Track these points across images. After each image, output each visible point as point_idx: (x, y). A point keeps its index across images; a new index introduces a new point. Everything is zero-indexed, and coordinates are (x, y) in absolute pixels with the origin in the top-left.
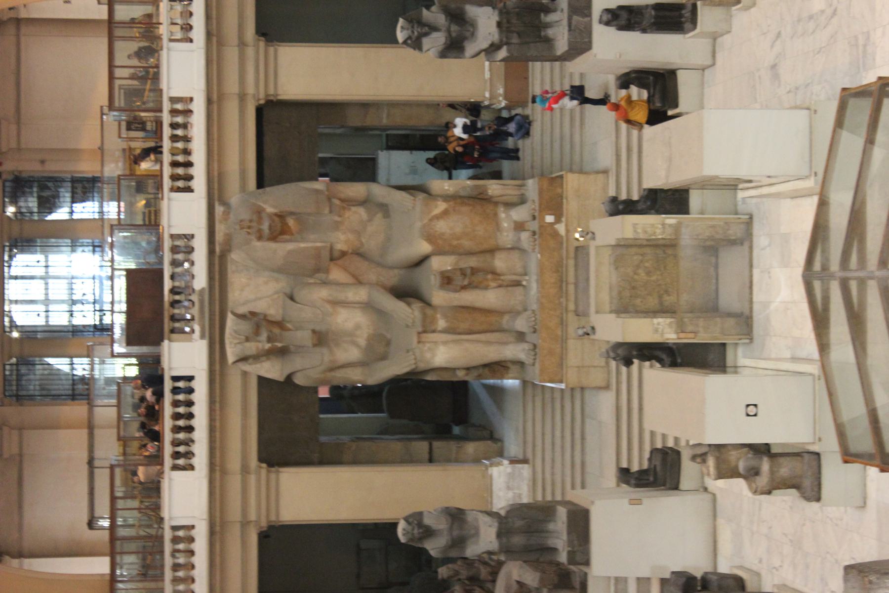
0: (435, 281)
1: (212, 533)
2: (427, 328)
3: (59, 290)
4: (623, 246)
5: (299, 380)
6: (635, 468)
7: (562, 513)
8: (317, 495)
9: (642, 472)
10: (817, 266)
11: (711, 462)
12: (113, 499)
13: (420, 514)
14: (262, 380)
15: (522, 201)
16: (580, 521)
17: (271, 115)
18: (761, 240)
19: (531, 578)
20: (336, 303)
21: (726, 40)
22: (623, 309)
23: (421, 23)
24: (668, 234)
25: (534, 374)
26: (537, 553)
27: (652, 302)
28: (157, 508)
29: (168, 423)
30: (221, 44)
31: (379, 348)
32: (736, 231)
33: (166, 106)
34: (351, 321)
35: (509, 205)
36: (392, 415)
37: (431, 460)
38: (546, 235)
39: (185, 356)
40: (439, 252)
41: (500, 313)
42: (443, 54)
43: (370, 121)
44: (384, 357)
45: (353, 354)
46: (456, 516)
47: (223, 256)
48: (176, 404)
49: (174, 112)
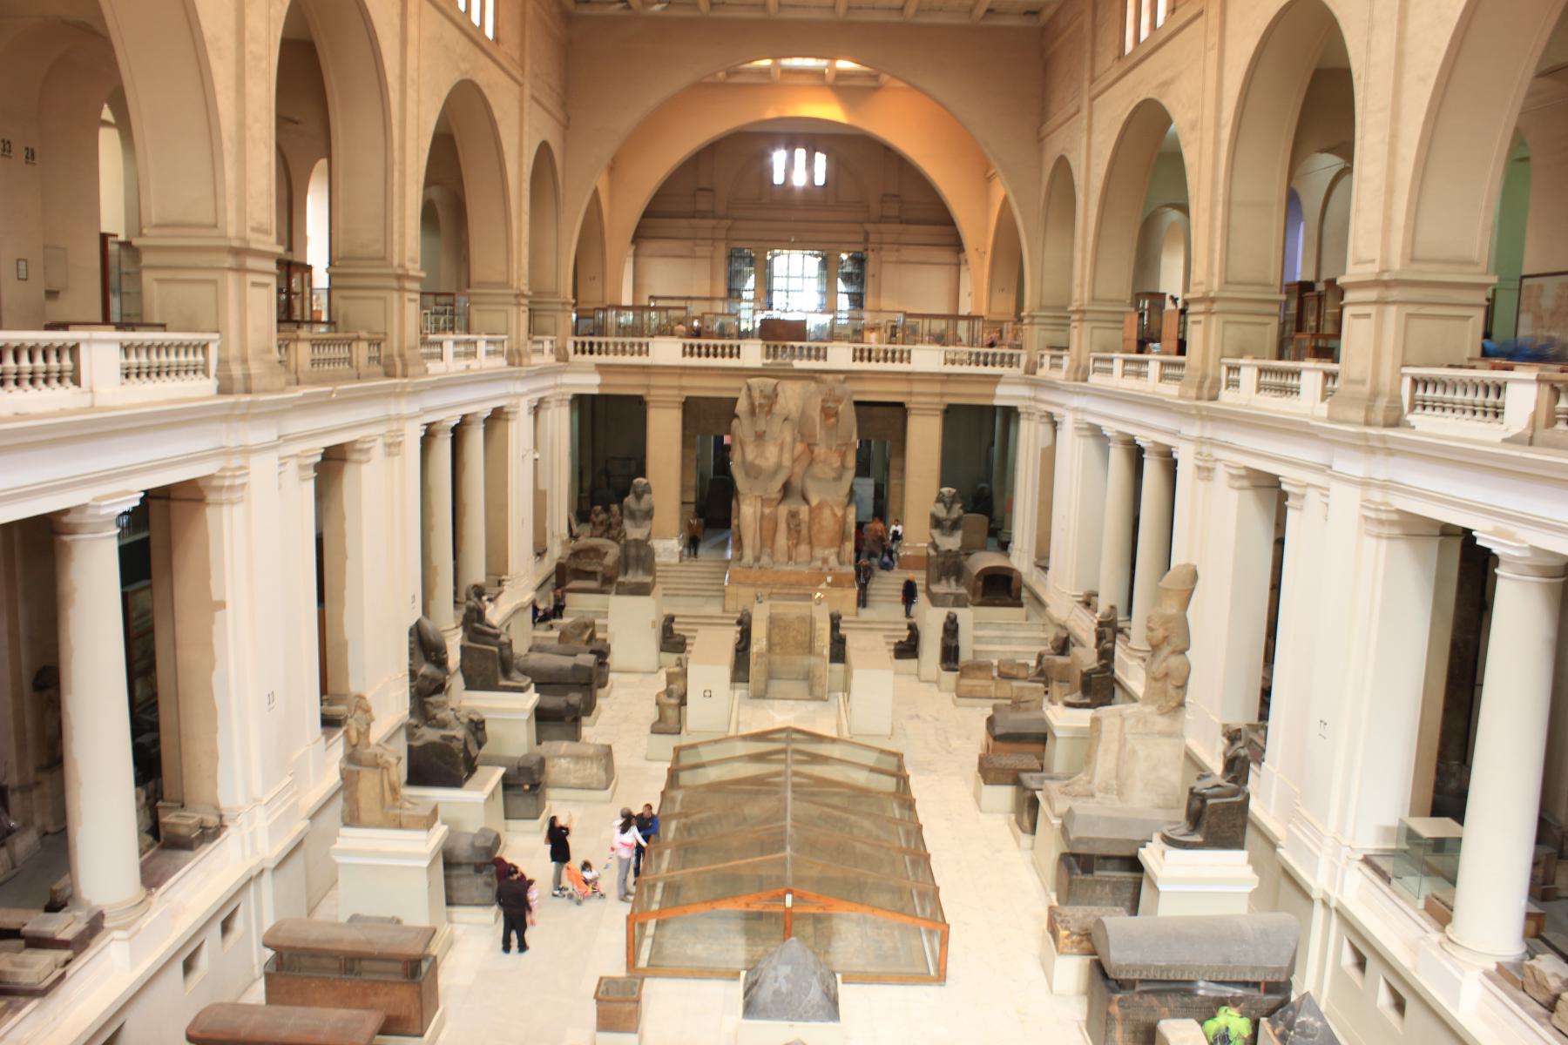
0: (793, 507)
2: (765, 502)
3: (795, 284)
4: (811, 622)
5: (735, 422)
6: (675, 626)
7: (648, 579)
8: (664, 434)
9: (671, 630)
10: (795, 736)
11: (677, 669)
12: (667, 309)
13: (649, 491)
14: (735, 400)
15: (841, 563)
16: (642, 590)
18: (812, 706)
19: (610, 560)
20: (782, 447)
21: (935, 688)
22: (773, 621)
23: (953, 502)
24: (817, 650)
25: (734, 567)
26: (624, 564)
27: (776, 639)
30: (942, 382)
31: (753, 472)
32: (818, 691)
33: (906, 347)
34: (770, 456)
35: (839, 555)
36: (712, 481)
37: (683, 503)
38: (818, 577)
39: (752, 354)
40: (811, 511)
43: (893, 472)
44: (747, 475)
46: (648, 514)
47: (812, 378)
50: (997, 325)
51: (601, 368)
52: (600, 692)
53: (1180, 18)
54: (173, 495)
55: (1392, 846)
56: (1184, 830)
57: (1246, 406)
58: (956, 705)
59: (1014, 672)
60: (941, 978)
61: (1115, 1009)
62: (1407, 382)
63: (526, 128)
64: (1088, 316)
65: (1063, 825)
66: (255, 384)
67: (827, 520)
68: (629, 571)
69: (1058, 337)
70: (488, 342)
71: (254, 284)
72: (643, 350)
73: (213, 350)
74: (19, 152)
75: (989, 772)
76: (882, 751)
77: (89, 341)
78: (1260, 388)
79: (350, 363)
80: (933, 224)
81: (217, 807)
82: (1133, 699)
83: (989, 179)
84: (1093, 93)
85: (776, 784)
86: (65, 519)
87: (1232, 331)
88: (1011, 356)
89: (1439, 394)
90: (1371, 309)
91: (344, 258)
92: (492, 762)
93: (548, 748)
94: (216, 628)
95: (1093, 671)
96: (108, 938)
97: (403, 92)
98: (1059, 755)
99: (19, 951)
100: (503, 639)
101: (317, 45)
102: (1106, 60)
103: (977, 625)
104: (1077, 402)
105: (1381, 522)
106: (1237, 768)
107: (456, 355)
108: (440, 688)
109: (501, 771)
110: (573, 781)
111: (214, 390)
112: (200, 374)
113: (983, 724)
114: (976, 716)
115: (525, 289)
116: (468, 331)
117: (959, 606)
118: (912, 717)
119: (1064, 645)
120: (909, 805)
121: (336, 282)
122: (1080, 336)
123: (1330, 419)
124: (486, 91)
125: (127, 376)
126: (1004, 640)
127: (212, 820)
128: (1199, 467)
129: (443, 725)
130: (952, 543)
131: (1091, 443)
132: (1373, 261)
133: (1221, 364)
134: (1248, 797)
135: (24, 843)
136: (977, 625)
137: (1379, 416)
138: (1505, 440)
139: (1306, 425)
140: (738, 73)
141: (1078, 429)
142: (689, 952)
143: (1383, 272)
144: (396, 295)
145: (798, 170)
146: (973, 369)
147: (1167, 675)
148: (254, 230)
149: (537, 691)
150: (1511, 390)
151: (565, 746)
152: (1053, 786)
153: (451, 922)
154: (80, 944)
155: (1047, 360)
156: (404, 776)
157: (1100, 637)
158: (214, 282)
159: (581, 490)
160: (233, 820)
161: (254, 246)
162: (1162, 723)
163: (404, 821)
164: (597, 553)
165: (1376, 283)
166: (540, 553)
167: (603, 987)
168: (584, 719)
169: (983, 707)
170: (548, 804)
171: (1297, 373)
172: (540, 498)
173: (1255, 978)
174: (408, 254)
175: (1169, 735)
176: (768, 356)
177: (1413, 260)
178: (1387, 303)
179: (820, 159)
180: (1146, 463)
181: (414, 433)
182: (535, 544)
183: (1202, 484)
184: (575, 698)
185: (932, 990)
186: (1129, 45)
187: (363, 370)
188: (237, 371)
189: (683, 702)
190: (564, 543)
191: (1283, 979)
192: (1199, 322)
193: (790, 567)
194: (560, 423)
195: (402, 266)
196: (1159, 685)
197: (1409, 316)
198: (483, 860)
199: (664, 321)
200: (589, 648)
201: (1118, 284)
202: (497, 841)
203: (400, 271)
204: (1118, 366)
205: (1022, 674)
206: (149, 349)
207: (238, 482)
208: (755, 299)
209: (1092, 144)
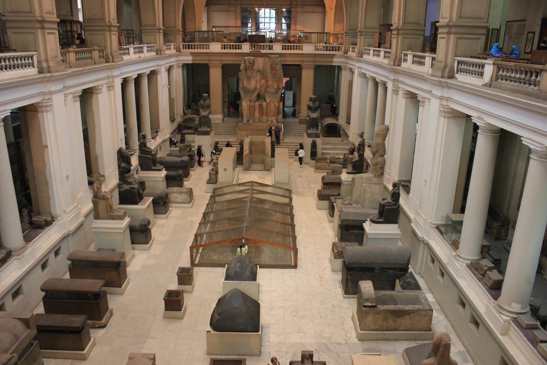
0: (261, 103)
1: (208, 53)
2: (250, 101)
3: (267, 20)
4: (263, 143)
5: (240, 73)
7: (209, 129)
8: (216, 76)
9: (218, 147)
14: (240, 64)
15: (278, 122)
16: (207, 133)
17: (299, 67)
18: (265, 172)
19: (197, 122)
21: (309, 166)
22: (251, 143)
26: (200, 124)
27: (253, 149)
29: (231, 44)
31: (247, 91)
32: (267, 168)
34: (253, 84)
35: (277, 120)
37: (223, 101)
40: (267, 104)
41: (253, 117)
42: (308, 106)
44: (244, 91)
45: (245, 85)
46: (209, 107)
47: (267, 57)
48: (236, 45)
50: (336, 36)
51: (192, 54)
52: (191, 169)
56: (376, 218)
57: (409, 69)
59: (335, 161)
60: (295, 267)
61: (349, 277)
62: (456, 62)
64: (363, 34)
66: (52, 69)
68: (204, 126)
70: (148, 47)
71: (48, 33)
72: (208, 47)
73: (35, 58)
75: (321, 197)
76: (286, 190)
78: (413, 62)
79: (92, 59)
81: (51, 214)
85: (245, 201)
88: (339, 47)
90: (445, 36)
92: (149, 195)
93: (171, 189)
94: (45, 155)
95: (356, 161)
96: (14, 258)
100: (153, 153)
103: (323, 144)
104: (358, 65)
105: (445, 112)
106: (396, 196)
107: (135, 53)
108: (129, 171)
109: (152, 198)
110: (179, 200)
112: (31, 67)
114: (320, 176)
115: (161, 27)
117: (317, 137)
118: (299, 177)
120: (292, 208)
122: (360, 40)
127: (49, 219)
129: (130, 183)
130: (315, 115)
131: (363, 79)
132: (447, 18)
136: (323, 144)
137: (446, 74)
138: (483, 85)
139: (423, 76)
142: (212, 258)
143: (450, 22)
146: (325, 52)
147: (377, 164)
150: (486, 67)
151: (176, 189)
152: (339, 201)
155: (351, 48)
156: (118, 202)
159: (189, 97)
160: (57, 218)
161: (46, 19)
162: (375, 180)
164: (192, 120)
165: (448, 26)
166: (172, 120)
169: (324, 172)
170: (170, 208)
171: (424, 57)
172: (171, 102)
173: (396, 267)
174: (111, 17)
182: (170, 118)
183: (394, 96)
185: (292, 270)
187: (97, 61)
188: (44, 65)
190: (181, 116)
191: (405, 267)
194: (178, 75)
195: (109, 22)
196: (374, 167)
197: (458, 38)
199: (215, 36)
200: (187, 154)
201: (374, 22)
202: (149, 222)
203: (109, 24)
204: (372, 52)
205: (338, 161)
206: (9, 59)
207: (48, 104)
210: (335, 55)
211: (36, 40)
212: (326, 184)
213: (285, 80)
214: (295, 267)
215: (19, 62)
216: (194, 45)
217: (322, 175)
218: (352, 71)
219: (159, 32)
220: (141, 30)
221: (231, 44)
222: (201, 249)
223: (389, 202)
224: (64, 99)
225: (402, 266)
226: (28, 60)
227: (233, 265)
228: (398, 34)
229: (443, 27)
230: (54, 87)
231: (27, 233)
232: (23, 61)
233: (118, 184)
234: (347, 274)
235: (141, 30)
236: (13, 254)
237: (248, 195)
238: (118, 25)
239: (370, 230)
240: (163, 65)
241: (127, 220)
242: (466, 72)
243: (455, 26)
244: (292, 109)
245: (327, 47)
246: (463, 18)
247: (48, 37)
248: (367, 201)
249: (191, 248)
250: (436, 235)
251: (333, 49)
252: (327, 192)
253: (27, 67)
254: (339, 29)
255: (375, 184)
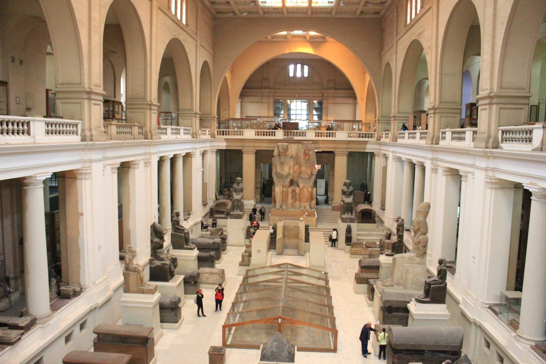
0: (294, 188)
1: (242, 139)
2: (284, 186)
3: (299, 112)
4: (297, 228)
5: (273, 158)
7: (242, 213)
8: (249, 162)
10: (289, 266)
14: (273, 151)
15: (311, 208)
16: (239, 217)
18: (298, 257)
19: (229, 207)
21: (343, 252)
22: (285, 228)
25: (273, 209)
26: (233, 209)
27: (286, 234)
28: (247, 128)
29: (265, 131)
30: (347, 144)
31: (280, 176)
32: (301, 252)
34: (286, 170)
35: (310, 205)
36: (267, 181)
37: (256, 188)
39: (280, 134)
40: (300, 190)
43: (331, 176)
44: (278, 177)
45: (279, 170)
46: (241, 190)
48: (269, 132)
49: (332, 133)
50: (368, 125)
51: (226, 140)
52: (223, 252)
53: (424, 10)
54: (66, 176)
55: (499, 303)
56: (422, 297)
57: (449, 145)
58: (350, 257)
60: (335, 350)
61: (396, 361)
62: (500, 132)
63: (198, 56)
65: (381, 296)
66: (94, 138)
67: (306, 193)
69: (387, 127)
70: (184, 130)
71: (94, 104)
73: (80, 126)
74: (17, 62)
75: (359, 280)
77: (34, 121)
78: (453, 139)
79: (131, 134)
80: (346, 90)
81: (80, 285)
82: (409, 251)
83: (365, 73)
84: (397, 39)
86: (25, 181)
87: (443, 119)
88: (372, 134)
89: (511, 135)
90: (487, 107)
91: (131, 98)
94: (80, 223)
95: (396, 243)
97: (151, 41)
98: (382, 271)
99: (6, 330)
100: (186, 231)
101: (122, 25)
102: (401, 27)
103: (358, 230)
105: (492, 183)
106: (442, 274)
107: (172, 133)
108: (161, 247)
109: (183, 277)
111: (80, 140)
112: (75, 134)
113: (358, 262)
115: (198, 111)
116: (178, 125)
118: (334, 261)
119: (389, 237)
120: (328, 290)
121: (128, 107)
123: (475, 147)
124: (183, 43)
125: (48, 133)
126: (368, 235)
127: (78, 289)
128: (432, 169)
129: (162, 260)
130: (349, 200)
131: (398, 163)
133: (439, 131)
134: (446, 284)
135: (15, 297)
136: (358, 230)
137: (490, 145)
138: (533, 150)
139: (466, 150)
140: (275, 37)
141: (394, 159)
142: (245, 339)
143: (491, 93)
144: (148, 111)
145: (298, 71)
147: (419, 242)
148: (94, 85)
149: (198, 249)
150: (535, 132)
151: (207, 270)
152: (379, 283)
153: (162, 328)
154: (27, 328)
155: (384, 135)
156: (149, 279)
157: (398, 230)
158: (80, 103)
159: (221, 184)
160: (85, 289)
161: (94, 91)
162: (418, 260)
163: (145, 291)
164: (225, 205)
166: (205, 204)
167: (212, 349)
168: (216, 261)
171: (464, 133)
173: (448, 349)
174: (153, 97)
175: (421, 264)
176: (285, 135)
177: (501, 88)
178: (492, 104)
179: (306, 68)
180: (416, 169)
181: (155, 160)
182: (203, 202)
183: (434, 175)
184: (213, 253)
185: (332, 354)
186: (408, 21)
188: (88, 133)
189: (250, 256)
190: (214, 201)
191: (457, 350)
192: (432, 117)
193: (293, 209)
194: (212, 160)
195: (151, 101)
196: (417, 246)
197: (500, 108)
198: (174, 306)
199: (249, 124)
201: (407, 107)
202: (179, 300)
203: (150, 103)
206: (56, 124)
207: (88, 171)
208: (284, 117)
209: (397, 58)
210: (368, 141)
211: (82, 110)
212: (364, 268)
213: (318, 167)
214: (335, 350)
215: (65, 128)
216: (229, 132)
217: (359, 259)
218: (386, 157)
219: (196, 117)
220: (178, 114)
221: (265, 131)
222: (234, 328)
223: (435, 280)
224: (102, 169)
225: (455, 349)
226: (73, 127)
227: (269, 344)
228: (435, 113)
229: (483, 98)
230: (96, 155)
231: (54, 303)
232: (68, 128)
233: (150, 260)
234: (394, 357)
235: (178, 114)
236: (37, 322)
237: (282, 276)
238: (158, 104)
239: (415, 310)
240: (198, 149)
241: (156, 296)
242: (512, 140)
243: (497, 97)
244: (325, 197)
245: (360, 134)
246: (505, 88)
247: (94, 108)
248: (410, 282)
249: (224, 327)
250: (490, 316)
251: (366, 136)
252: (365, 275)
253: (72, 134)
254: (370, 118)
255: (417, 263)
